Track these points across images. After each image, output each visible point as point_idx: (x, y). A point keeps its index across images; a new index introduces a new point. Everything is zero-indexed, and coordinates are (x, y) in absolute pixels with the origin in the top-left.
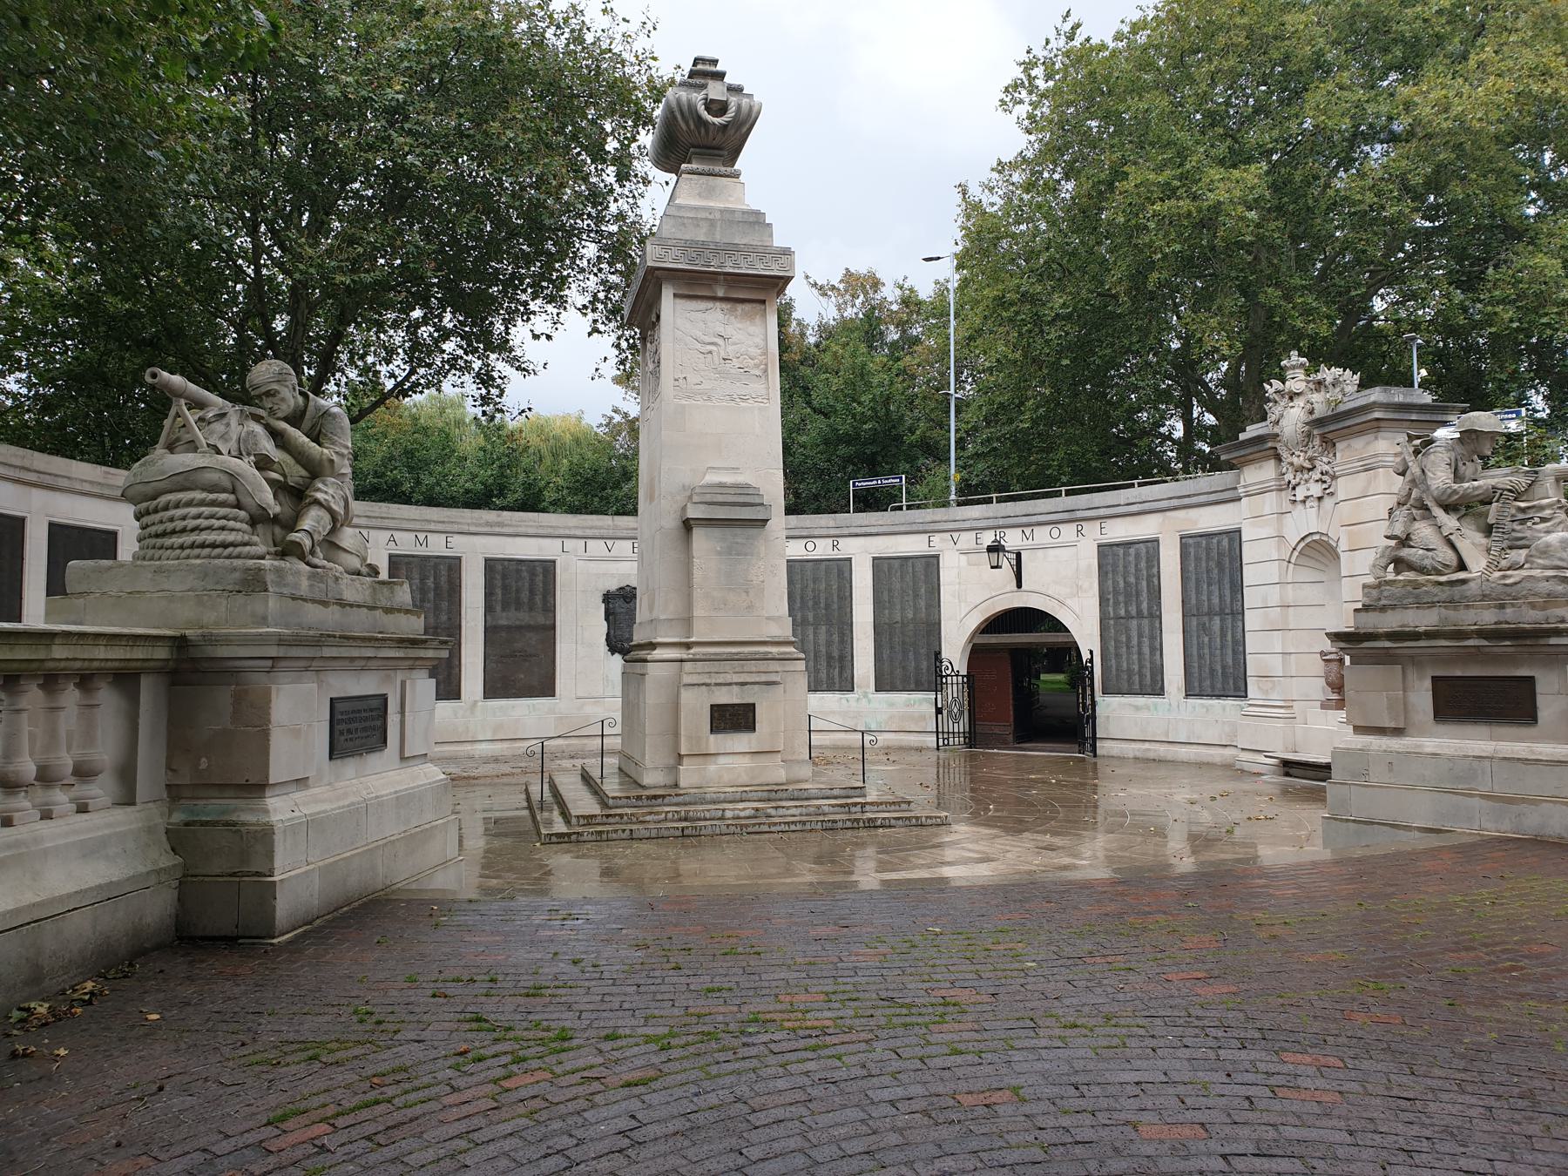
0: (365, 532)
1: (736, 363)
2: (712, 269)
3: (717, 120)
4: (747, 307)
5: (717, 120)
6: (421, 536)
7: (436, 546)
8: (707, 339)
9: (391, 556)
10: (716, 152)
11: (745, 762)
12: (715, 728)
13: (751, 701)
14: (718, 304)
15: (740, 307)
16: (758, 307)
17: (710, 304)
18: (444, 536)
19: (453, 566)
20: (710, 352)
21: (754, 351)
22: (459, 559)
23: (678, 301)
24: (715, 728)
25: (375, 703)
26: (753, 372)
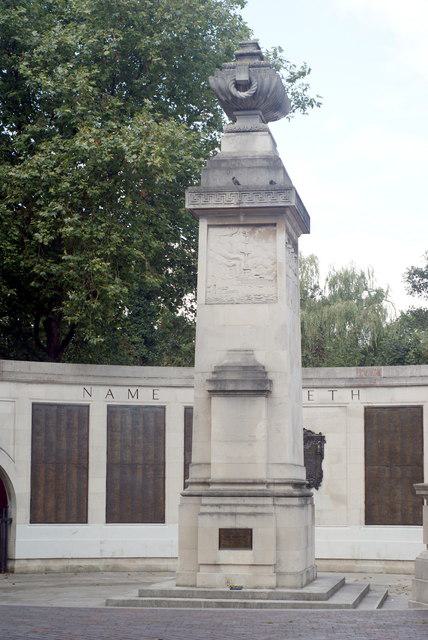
0: (88, 388)
1: (254, 272)
2: (232, 206)
3: (243, 95)
4: (263, 229)
5: (243, 95)
6: (133, 390)
7: (145, 398)
8: (232, 256)
9: (109, 406)
10: (253, 112)
11: (245, 572)
12: (222, 546)
13: (249, 527)
14: (241, 229)
15: (258, 231)
16: (272, 228)
17: (235, 230)
18: (150, 390)
19: (160, 413)
20: (234, 265)
21: (269, 263)
22: (164, 408)
23: (211, 229)
24: (222, 546)
25: (84, 519)
26: (267, 277)
